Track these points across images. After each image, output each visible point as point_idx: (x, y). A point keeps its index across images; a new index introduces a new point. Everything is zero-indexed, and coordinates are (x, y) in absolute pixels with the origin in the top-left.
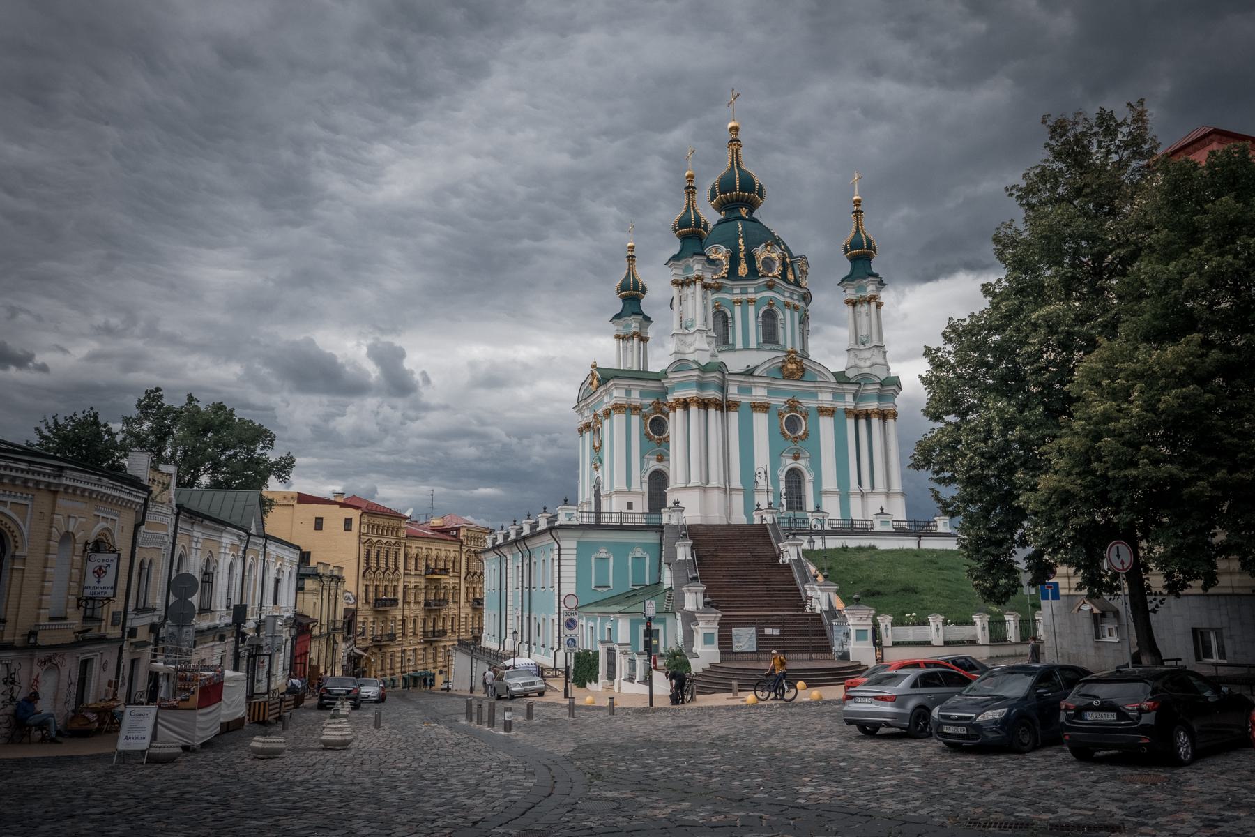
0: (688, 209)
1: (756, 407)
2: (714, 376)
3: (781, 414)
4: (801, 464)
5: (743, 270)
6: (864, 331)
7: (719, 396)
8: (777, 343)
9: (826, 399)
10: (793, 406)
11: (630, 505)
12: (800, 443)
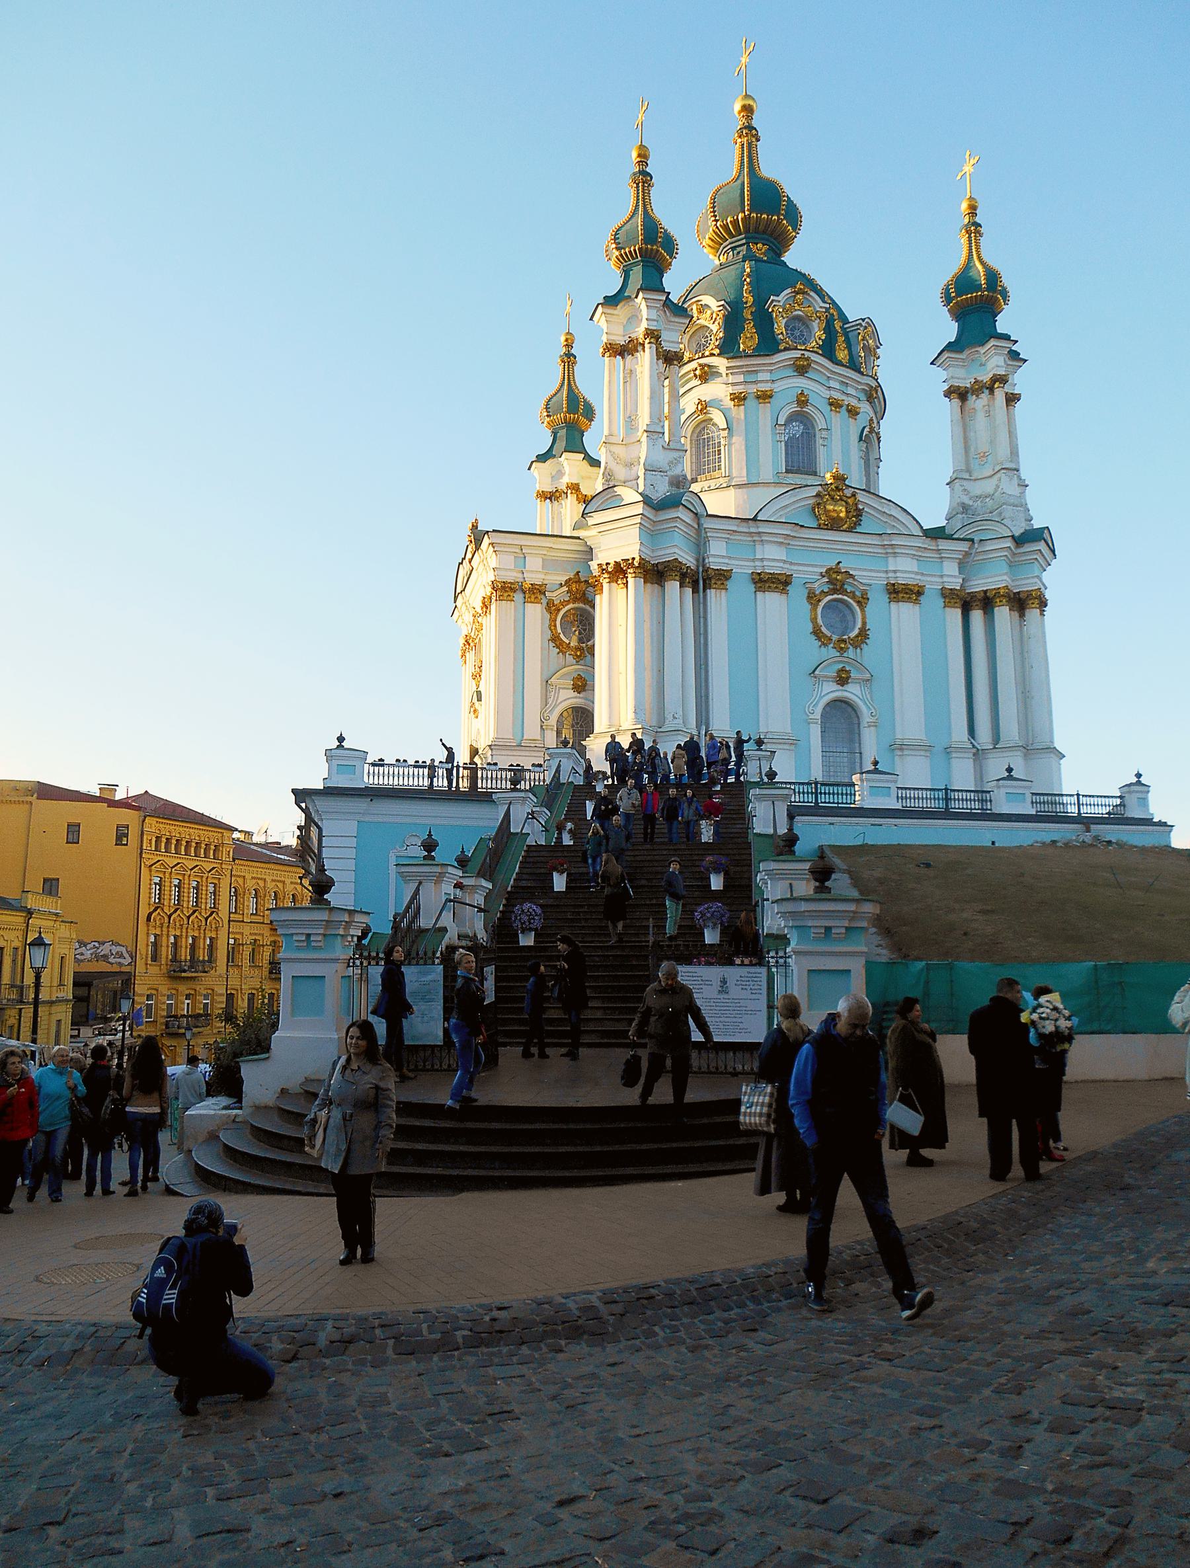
4: (852, 692)
5: (748, 339)
9: (905, 569)
10: (837, 579)
12: (851, 653)
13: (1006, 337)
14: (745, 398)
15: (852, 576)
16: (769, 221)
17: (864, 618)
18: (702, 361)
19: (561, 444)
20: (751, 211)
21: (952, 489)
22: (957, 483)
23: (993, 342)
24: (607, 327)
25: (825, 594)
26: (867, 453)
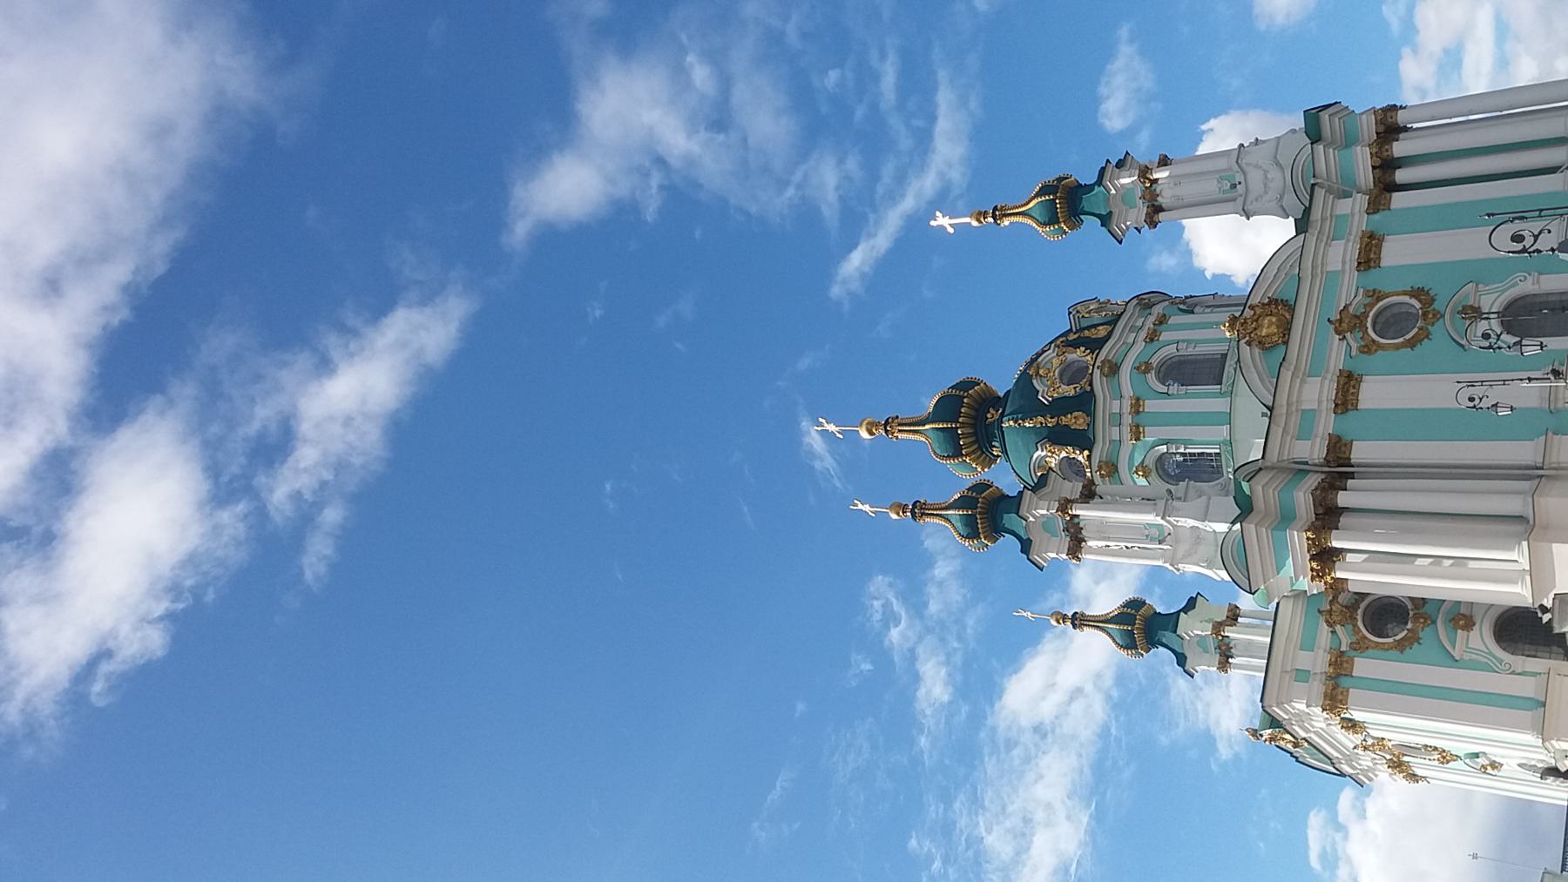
0: (947, 519)
1: (1346, 399)
2: (1262, 491)
3: (1368, 348)
4: (1492, 300)
5: (1076, 421)
6: (1211, 187)
7: (1313, 481)
8: (1225, 356)
10: (1347, 323)
13: (1102, 171)
14: (1137, 426)
18: (1095, 468)
19: (1167, 637)
21: (1255, 214)
22: (1249, 207)
24: (1053, 553)
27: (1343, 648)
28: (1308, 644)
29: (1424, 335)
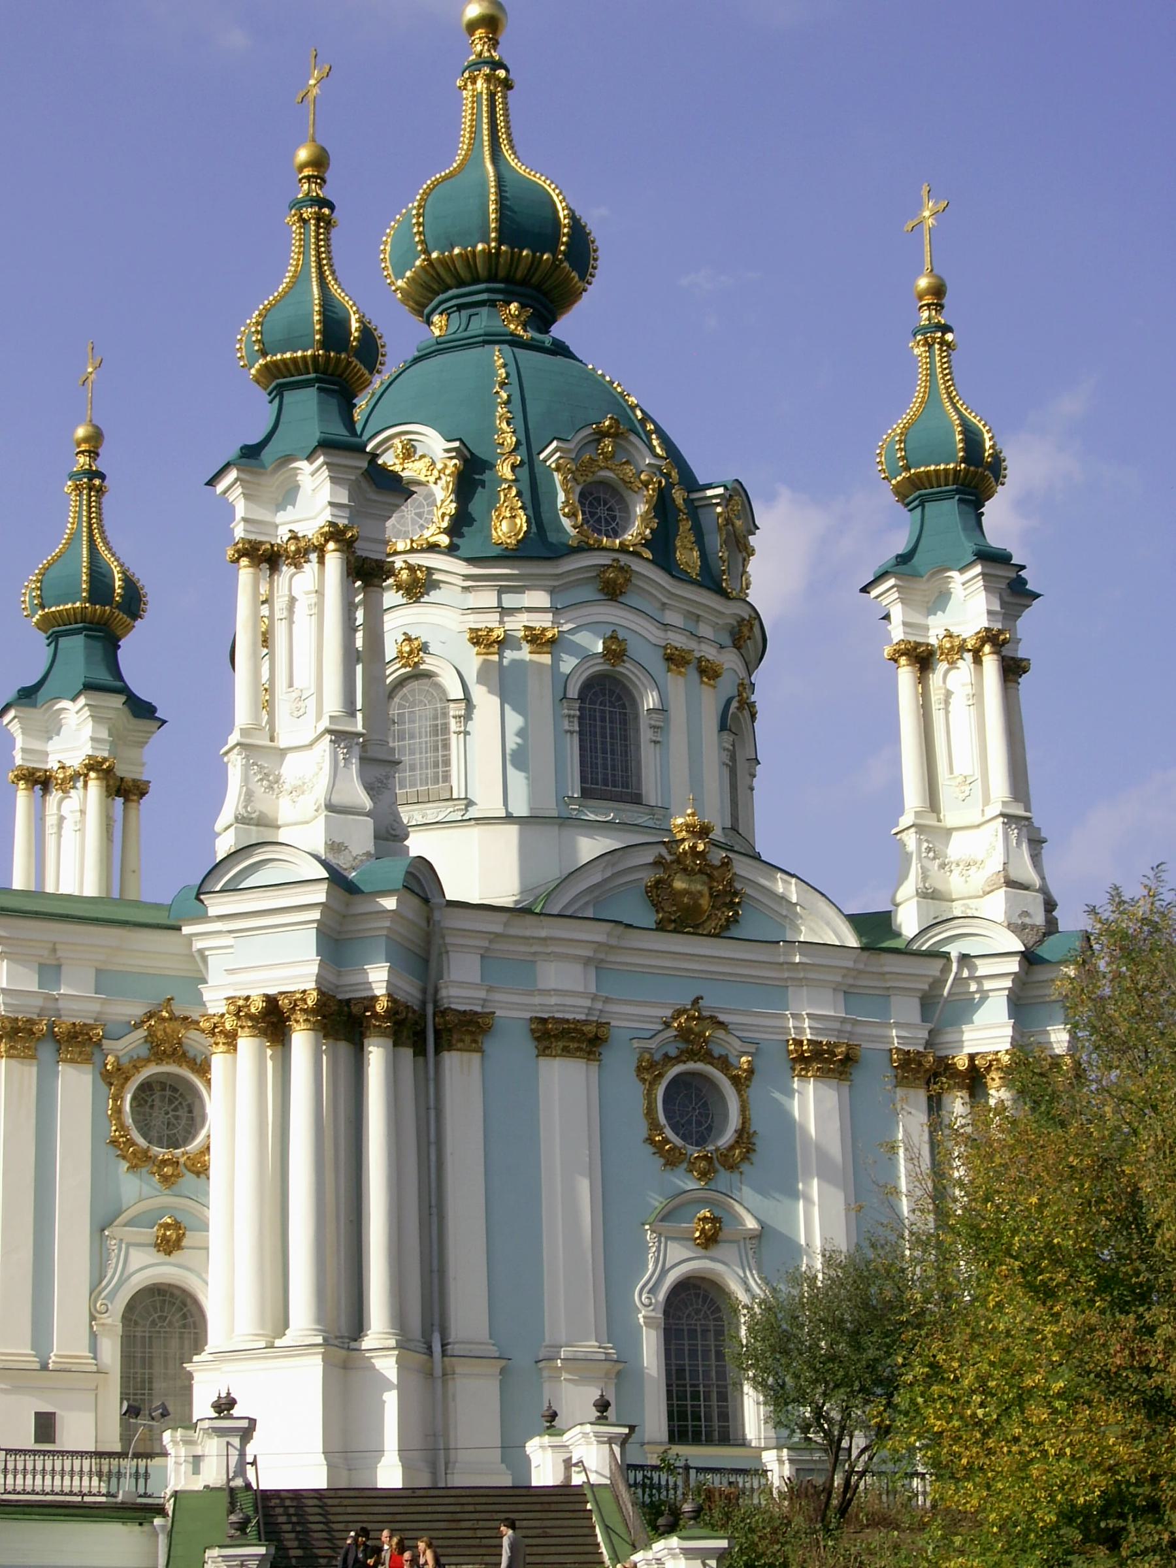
0: (300, 279)
3: (649, 1069)
7: (410, 992)
11: (45, 1426)
15: (722, 1025)
16: (535, 263)
17: (744, 1109)
18: (414, 559)
20: (500, 241)
23: (978, 569)
25: (668, 1060)
26: (733, 758)
27: (106, 1044)
28: (105, 980)
29: (672, 1159)
